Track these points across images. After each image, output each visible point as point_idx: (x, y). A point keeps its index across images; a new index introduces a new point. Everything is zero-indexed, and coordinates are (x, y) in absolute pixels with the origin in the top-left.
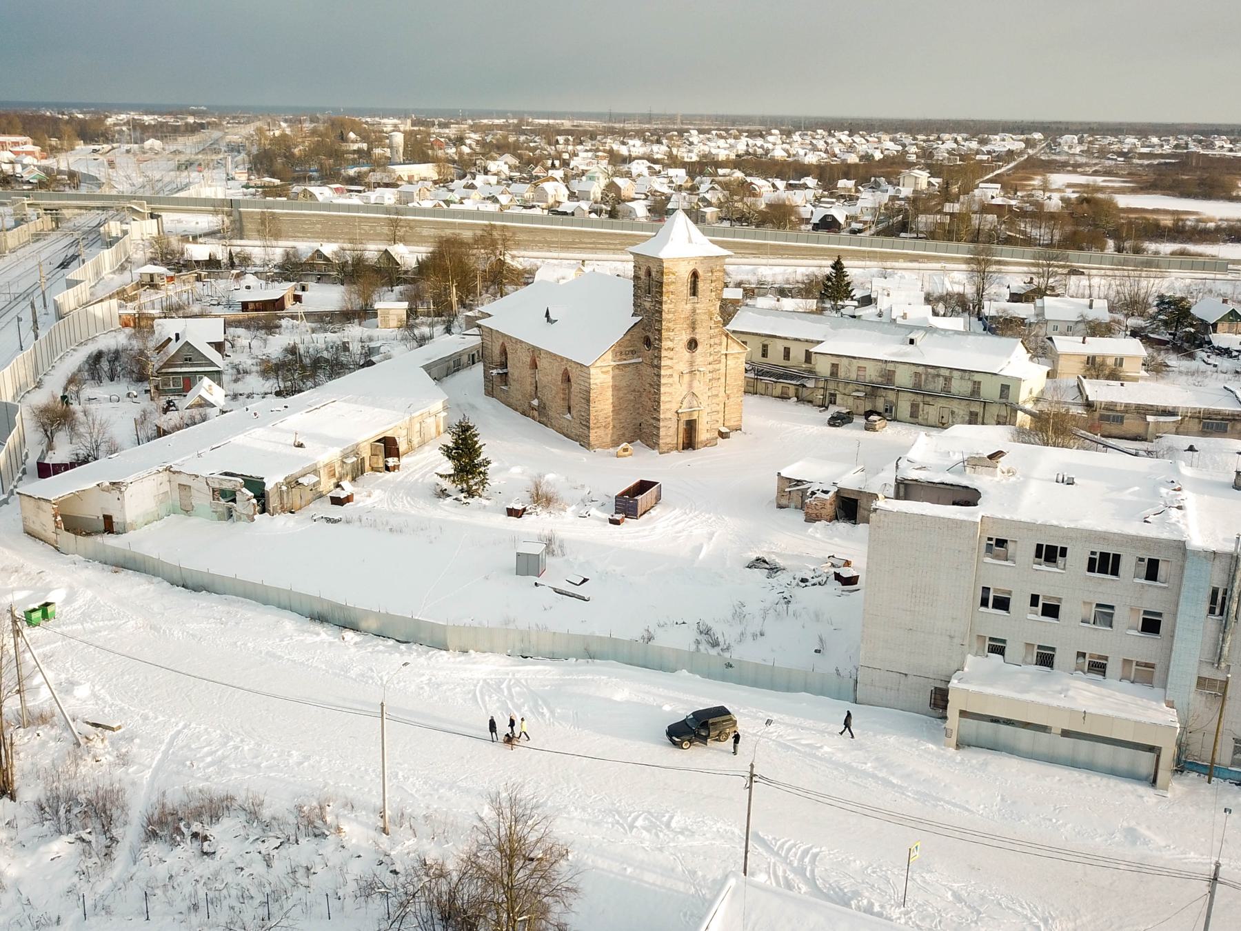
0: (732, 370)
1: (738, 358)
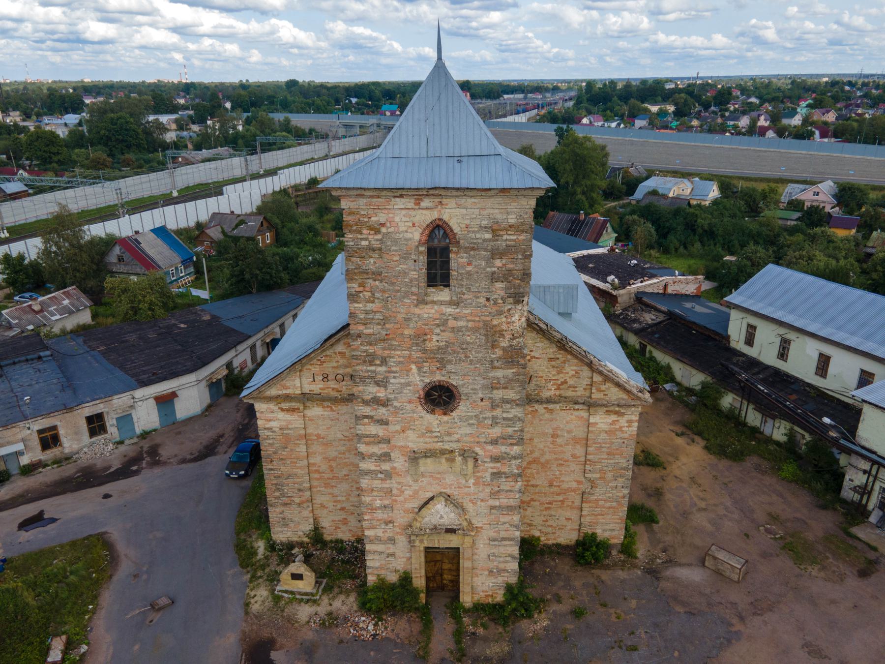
0: (604, 436)
1: (616, 413)
